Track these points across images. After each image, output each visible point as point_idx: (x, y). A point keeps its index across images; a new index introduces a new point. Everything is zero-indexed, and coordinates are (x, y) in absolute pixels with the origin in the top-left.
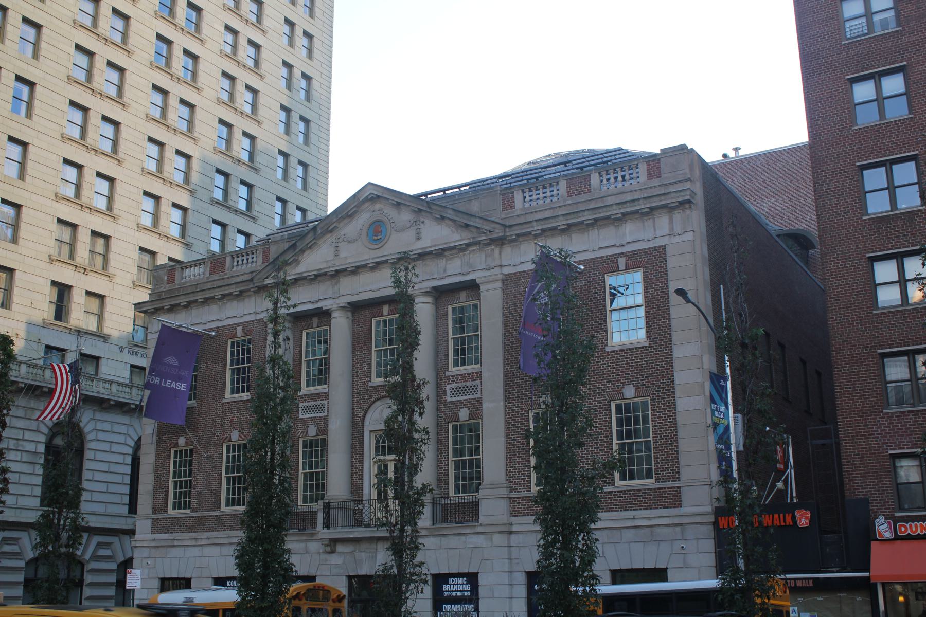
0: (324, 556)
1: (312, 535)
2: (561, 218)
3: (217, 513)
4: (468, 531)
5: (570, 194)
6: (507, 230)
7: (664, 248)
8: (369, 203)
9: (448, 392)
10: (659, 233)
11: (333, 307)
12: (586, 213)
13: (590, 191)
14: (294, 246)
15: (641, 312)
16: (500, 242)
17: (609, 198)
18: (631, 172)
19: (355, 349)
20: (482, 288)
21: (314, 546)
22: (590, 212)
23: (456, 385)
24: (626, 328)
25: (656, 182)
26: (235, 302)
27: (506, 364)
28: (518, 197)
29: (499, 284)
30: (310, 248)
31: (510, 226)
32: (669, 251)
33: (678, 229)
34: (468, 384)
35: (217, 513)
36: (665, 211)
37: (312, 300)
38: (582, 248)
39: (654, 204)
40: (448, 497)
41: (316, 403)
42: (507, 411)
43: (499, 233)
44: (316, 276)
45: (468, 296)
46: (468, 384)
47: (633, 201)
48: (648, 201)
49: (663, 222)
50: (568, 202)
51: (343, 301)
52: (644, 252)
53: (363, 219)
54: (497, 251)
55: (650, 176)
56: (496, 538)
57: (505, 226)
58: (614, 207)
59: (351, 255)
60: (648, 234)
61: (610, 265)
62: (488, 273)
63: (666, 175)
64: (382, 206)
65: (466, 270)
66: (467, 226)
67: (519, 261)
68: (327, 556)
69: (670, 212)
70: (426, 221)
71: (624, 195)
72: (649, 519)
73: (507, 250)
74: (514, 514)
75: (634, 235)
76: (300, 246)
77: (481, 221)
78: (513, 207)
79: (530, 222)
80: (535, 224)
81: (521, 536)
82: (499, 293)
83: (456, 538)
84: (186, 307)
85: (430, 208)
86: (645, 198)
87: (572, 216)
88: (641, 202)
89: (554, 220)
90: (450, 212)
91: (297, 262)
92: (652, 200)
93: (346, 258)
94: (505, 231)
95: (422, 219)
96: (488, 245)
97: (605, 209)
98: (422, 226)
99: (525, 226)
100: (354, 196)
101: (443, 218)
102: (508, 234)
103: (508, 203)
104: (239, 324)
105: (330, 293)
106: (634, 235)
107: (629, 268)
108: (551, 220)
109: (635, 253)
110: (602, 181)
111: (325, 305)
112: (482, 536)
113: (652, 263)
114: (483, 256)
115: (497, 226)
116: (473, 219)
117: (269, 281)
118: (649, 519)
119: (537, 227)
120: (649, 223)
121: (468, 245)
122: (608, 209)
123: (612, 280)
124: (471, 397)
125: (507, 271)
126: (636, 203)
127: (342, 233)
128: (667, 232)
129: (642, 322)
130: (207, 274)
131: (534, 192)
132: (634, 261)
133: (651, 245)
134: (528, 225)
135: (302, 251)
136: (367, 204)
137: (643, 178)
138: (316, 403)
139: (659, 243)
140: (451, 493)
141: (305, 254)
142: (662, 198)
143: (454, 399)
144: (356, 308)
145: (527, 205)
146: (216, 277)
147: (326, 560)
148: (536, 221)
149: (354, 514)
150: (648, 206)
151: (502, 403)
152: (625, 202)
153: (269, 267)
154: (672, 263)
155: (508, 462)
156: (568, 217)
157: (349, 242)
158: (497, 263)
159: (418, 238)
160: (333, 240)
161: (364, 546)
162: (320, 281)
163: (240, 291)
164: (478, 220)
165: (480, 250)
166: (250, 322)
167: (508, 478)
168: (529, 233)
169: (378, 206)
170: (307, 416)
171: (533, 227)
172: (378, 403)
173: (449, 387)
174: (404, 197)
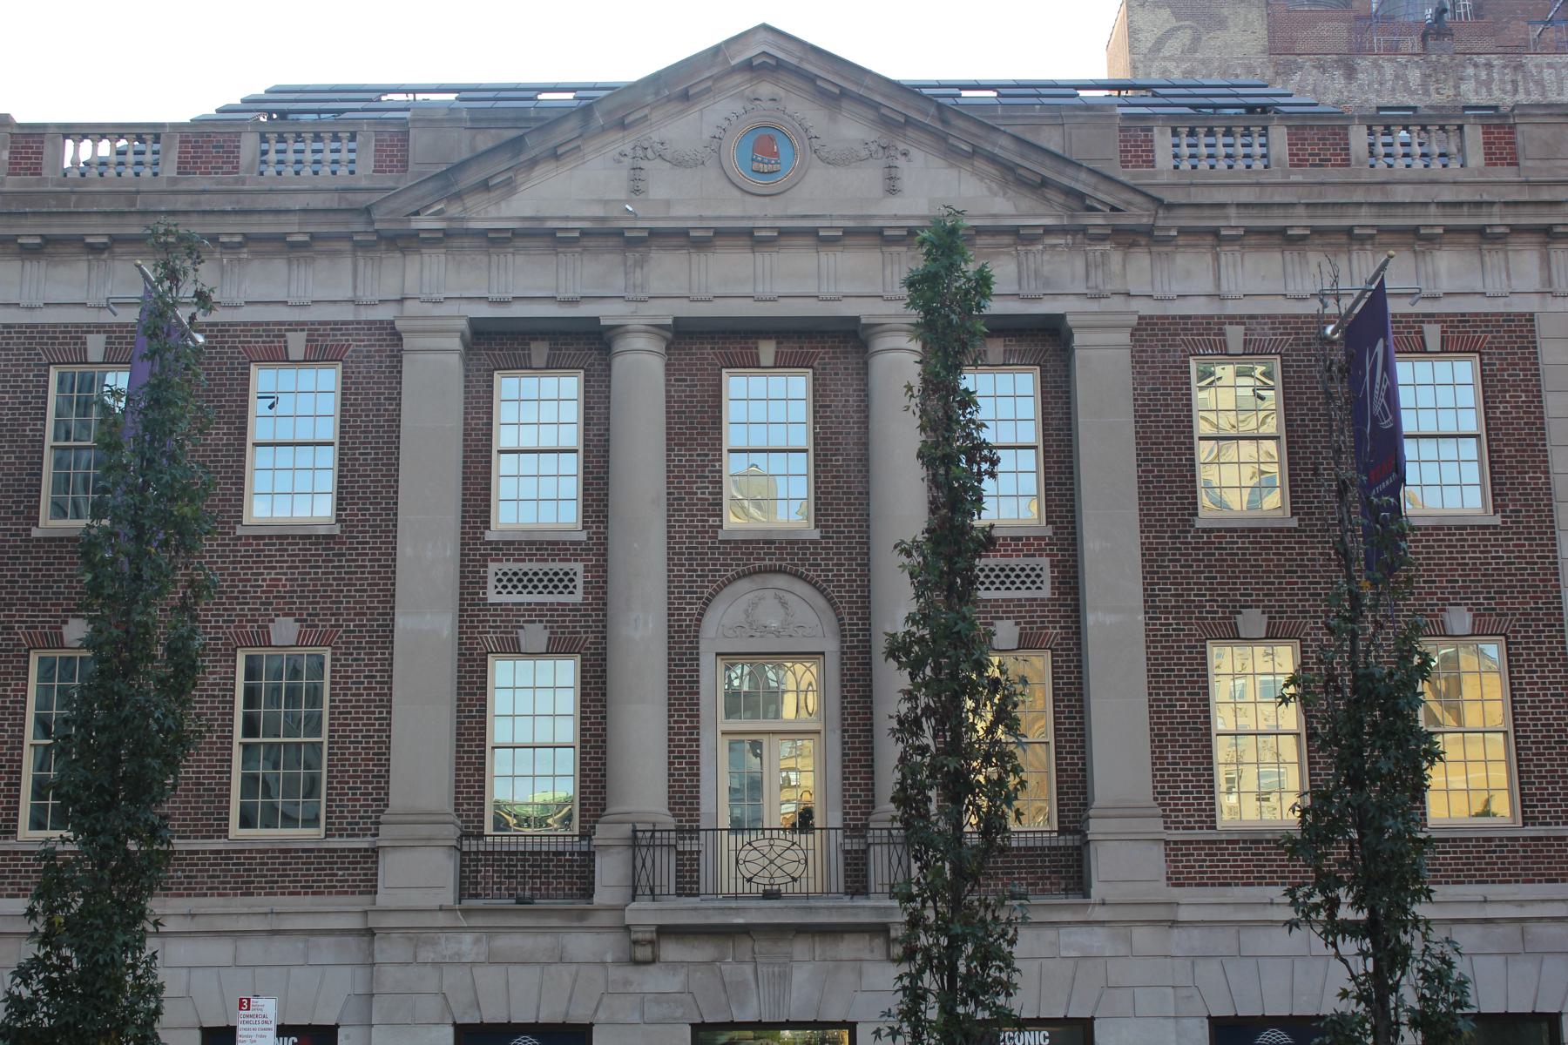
0: (617, 973)
1: (583, 914)
2: (1301, 211)
3: (218, 844)
4: (1067, 916)
5: (1297, 162)
6: (1161, 212)
7: (1530, 318)
8: (747, 76)
9: (491, 581)
10: (1517, 285)
11: (635, 323)
12: (1364, 210)
13: (1346, 163)
14: (516, 145)
15: (328, 457)
16: (1127, 237)
17: (1400, 188)
18: (300, 146)
19: (674, 439)
20: (1078, 339)
21: (582, 944)
22: (1374, 210)
23: (515, 567)
24: (289, 487)
25: (1506, 173)
27: (1145, 527)
28: (1163, 142)
29: (1124, 337)
30: (555, 155)
31: (1170, 206)
32: (1543, 328)
34: (1013, 562)
35: (218, 844)
36: (1534, 239)
37: (562, 295)
38: (250, 291)
39: (324, 229)
40: (481, 836)
41: (546, 566)
42: (1152, 637)
43: (1138, 215)
44: (848, 232)
45: (1008, 353)
46: (1013, 562)
47: (1478, 204)
48: (1511, 210)
50: (1293, 178)
51: (666, 312)
52: (1485, 319)
53: (719, 111)
54: (1116, 257)
55: (1491, 159)
56: (1141, 935)
57: (1159, 202)
58: (1433, 209)
59: (680, 197)
60: (1495, 284)
62: (1093, 306)
63: (1529, 163)
64: (782, 93)
65: (1031, 288)
66: (1045, 183)
67: (1177, 289)
68: (631, 973)
69: (1545, 244)
70: (914, 152)
71: (1436, 188)
72: (1521, 903)
73: (1141, 260)
74: (1175, 880)
75: (325, 290)
76: (534, 146)
77: (1093, 180)
78: (1151, 163)
79: (1222, 206)
80: (1232, 211)
81: (1195, 932)
82: (1126, 355)
83: (1084, 929)
84: (95, 249)
85: (944, 122)
86: (1506, 204)
87: (1329, 211)
88: (1496, 209)
89: (1281, 212)
90: (1004, 141)
91: (510, 187)
92: (1522, 210)
93: (668, 203)
94: (1155, 218)
95: (902, 146)
96: (1102, 238)
97: (1409, 211)
98: (901, 162)
99: (1207, 212)
100: (716, 51)
101: (976, 152)
102: (1160, 223)
103: (1138, 149)
104: (98, 328)
105: (618, 284)
106: (325, 290)
107: (1448, 348)
108: (1276, 212)
109: (1464, 318)
110: (265, 153)
111: (607, 313)
112: (1098, 930)
114: (1079, 265)
115: (1138, 199)
116: (1070, 171)
117: (424, 223)
118: (1521, 903)
119: (1234, 221)
120: (1494, 259)
121: (1048, 230)
122: (1418, 210)
123: (263, 378)
124: (1024, 594)
126: (1485, 210)
127: (655, 137)
128: (1538, 287)
129: (328, 481)
130: (169, 169)
131: (1204, 140)
132: (323, 347)
133: (1498, 306)
134: (1216, 212)
135: (534, 163)
136: (737, 78)
137: (1476, 158)
138: (546, 566)
139: (1519, 306)
140: (488, 829)
141: (539, 171)
142: (1545, 210)
143: (504, 598)
144: (684, 336)
145: (1186, 165)
146: (200, 182)
147: (627, 983)
148: (1238, 205)
149: (680, 864)
150: (1510, 221)
151: (1141, 617)
152: (1460, 204)
153: (430, 186)
155: (1158, 758)
156: (1319, 211)
157: (679, 163)
158: (1117, 286)
159: (892, 191)
160: (628, 149)
161: (745, 945)
162: (585, 249)
163: (313, 236)
164: (1083, 176)
165: (1070, 248)
166: (337, 326)
167: (1159, 794)
168: (80, 239)
169: (766, 89)
170: (515, 598)
171: (1227, 218)
172: (743, 585)
173: (493, 567)
174: (868, 81)
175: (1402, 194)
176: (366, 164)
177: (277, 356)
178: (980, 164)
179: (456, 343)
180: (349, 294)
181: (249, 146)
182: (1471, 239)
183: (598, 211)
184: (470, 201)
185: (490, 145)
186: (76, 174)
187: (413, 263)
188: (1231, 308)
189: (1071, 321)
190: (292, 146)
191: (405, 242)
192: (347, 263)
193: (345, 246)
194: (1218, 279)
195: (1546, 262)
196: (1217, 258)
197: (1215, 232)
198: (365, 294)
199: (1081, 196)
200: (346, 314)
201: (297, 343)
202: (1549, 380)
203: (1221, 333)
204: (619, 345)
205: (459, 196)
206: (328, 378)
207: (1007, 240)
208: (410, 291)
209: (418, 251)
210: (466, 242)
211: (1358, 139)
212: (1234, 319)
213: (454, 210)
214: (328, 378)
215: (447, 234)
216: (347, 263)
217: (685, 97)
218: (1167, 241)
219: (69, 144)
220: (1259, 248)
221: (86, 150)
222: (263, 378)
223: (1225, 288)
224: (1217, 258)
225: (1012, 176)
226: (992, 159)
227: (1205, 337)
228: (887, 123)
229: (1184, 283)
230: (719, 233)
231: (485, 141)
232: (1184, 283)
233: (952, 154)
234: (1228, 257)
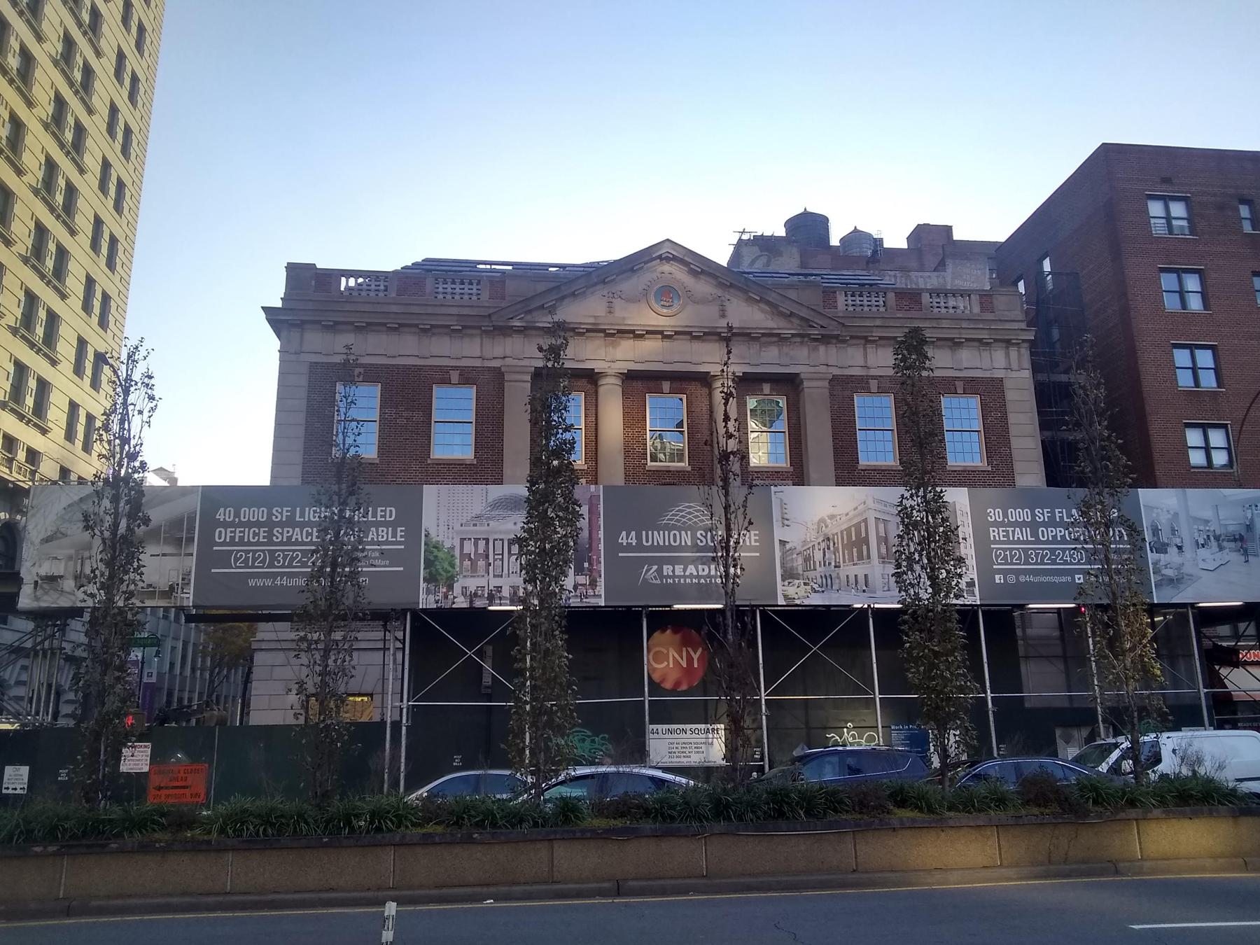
7: (1001, 380)
11: (610, 372)
16: (826, 339)
20: (806, 384)
26: (447, 339)
29: (826, 384)
30: (573, 294)
33: (1015, 365)
49: (999, 356)
51: (624, 367)
60: (986, 363)
61: (949, 386)
62: (812, 370)
66: (792, 314)
69: (1007, 348)
109: (973, 379)
111: (598, 366)
113: (990, 393)
120: (986, 354)
125: (837, 372)
135: (563, 298)
139: (999, 374)
141: (566, 301)
154: (1010, 396)
165: (802, 343)
175: (945, 324)
176: (485, 296)
177: (446, 381)
178: (763, 306)
179: (529, 378)
180: (478, 354)
181: (429, 283)
182: (976, 344)
183: (592, 320)
184: (535, 314)
185: (544, 289)
186: (347, 293)
187: (509, 341)
188: (873, 372)
189: (802, 376)
190: (449, 286)
191: (504, 331)
192: (478, 340)
193: (478, 332)
194: (866, 357)
195: (1007, 356)
196: (865, 349)
197: (865, 338)
198: (488, 354)
199: (807, 320)
200: (478, 363)
201: (455, 376)
202: (1010, 407)
203: (868, 383)
204: (601, 382)
205: (530, 312)
206: (472, 392)
207: (775, 339)
208: (508, 353)
209: (510, 336)
210: (534, 332)
211: (926, 298)
212: (874, 377)
213: (529, 317)
214: (472, 392)
215: (526, 328)
216: (478, 340)
217: (632, 270)
218: (844, 341)
219: (343, 279)
220: (884, 346)
221: (352, 282)
222: (437, 391)
223: (869, 364)
224: (865, 349)
225: (775, 310)
226: (768, 303)
227: (860, 384)
228: (721, 285)
229: (851, 360)
230: (648, 332)
231: (541, 287)
232: (851, 360)
233: (750, 300)
234: (871, 349)
